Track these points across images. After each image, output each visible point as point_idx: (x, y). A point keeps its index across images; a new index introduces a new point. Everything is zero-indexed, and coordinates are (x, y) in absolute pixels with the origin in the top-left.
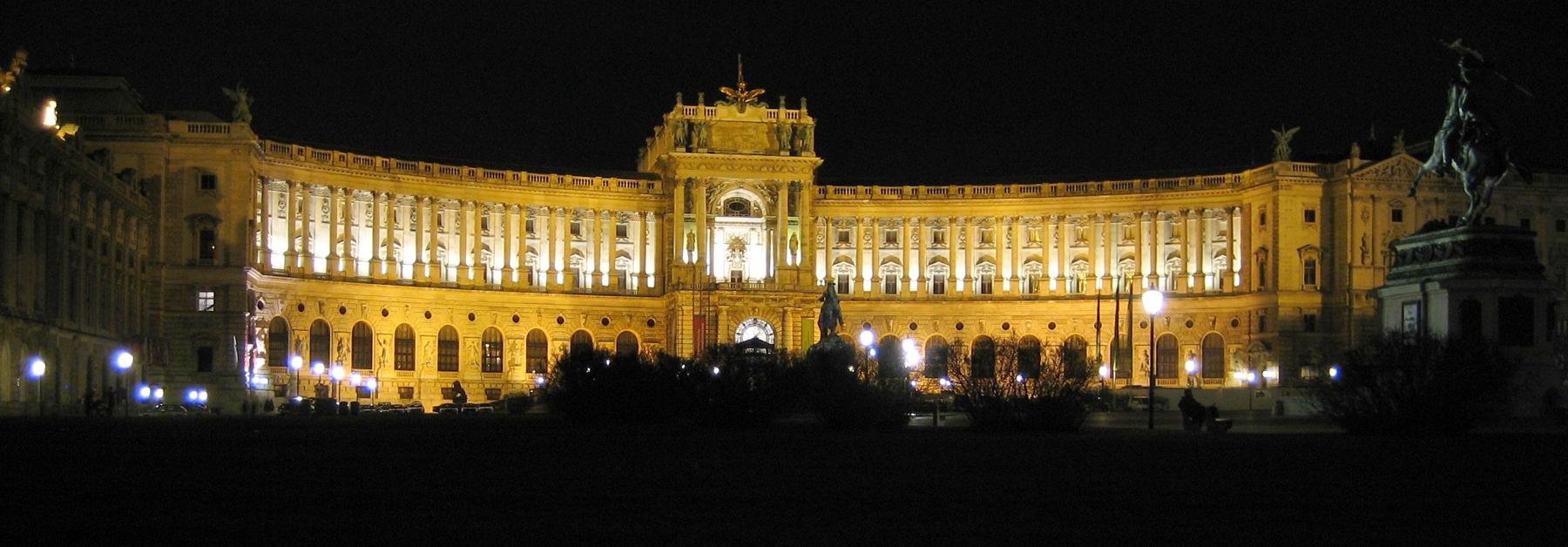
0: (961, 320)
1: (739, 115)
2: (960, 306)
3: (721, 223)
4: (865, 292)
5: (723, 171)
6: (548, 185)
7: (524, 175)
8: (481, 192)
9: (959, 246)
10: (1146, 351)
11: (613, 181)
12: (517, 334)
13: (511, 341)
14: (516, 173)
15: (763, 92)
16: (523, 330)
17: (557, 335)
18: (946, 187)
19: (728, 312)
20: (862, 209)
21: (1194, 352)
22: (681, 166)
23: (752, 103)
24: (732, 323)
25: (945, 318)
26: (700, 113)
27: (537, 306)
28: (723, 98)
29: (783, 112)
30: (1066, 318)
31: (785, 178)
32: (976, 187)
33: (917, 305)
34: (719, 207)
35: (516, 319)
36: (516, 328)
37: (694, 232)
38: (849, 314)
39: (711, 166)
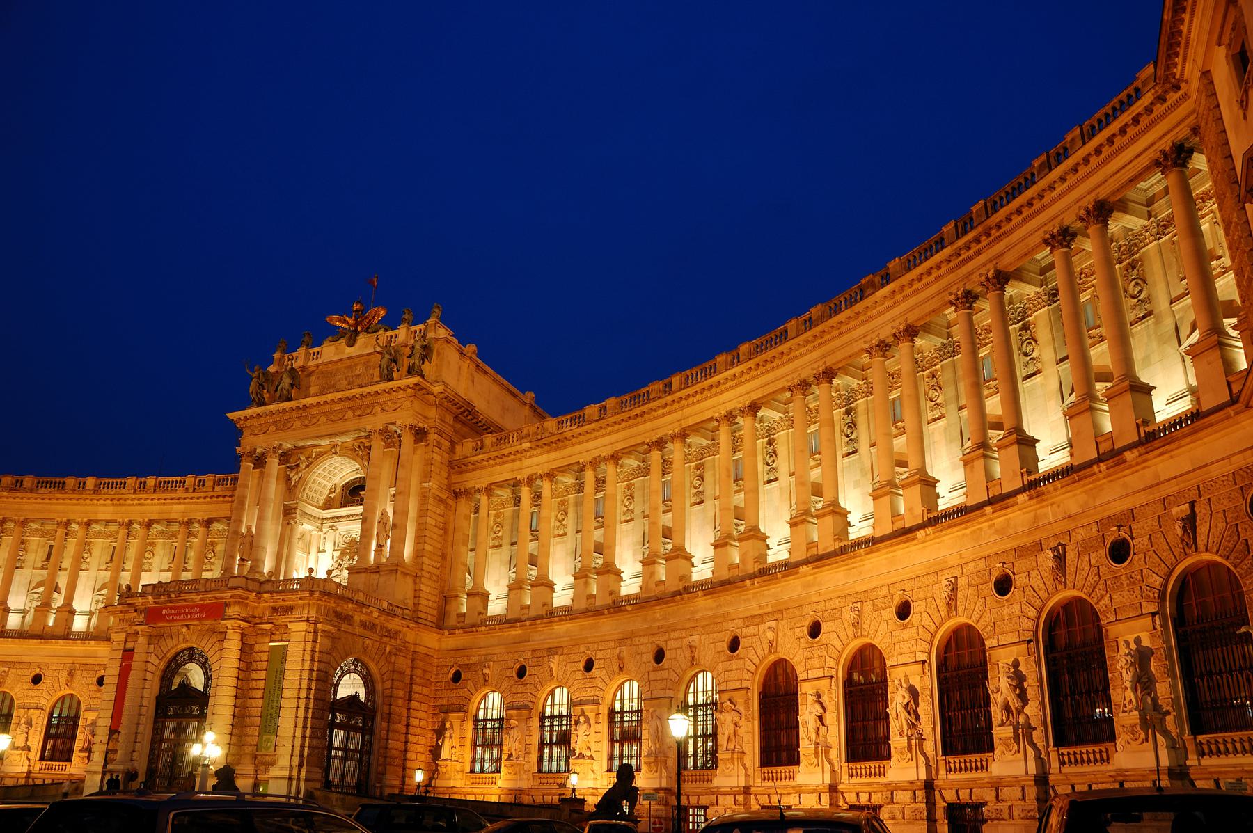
0: (659, 641)
1: (348, 350)
2: (658, 612)
3: (333, 518)
4: (523, 607)
5: (294, 430)
6: (124, 491)
7: (90, 482)
8: (25, 507)
9: (693, 500)
10: (1016, 664)
11: (209, 479)
12: (33, 702)
13: (22, 711)
14: (82, 480)
15: (382, 313)
16: (45, 697)
17: (94, 703)
18: (644, 390)
19: (150, 637)
20: (527, 462)
21: (1146, 642)
22: (246, 432)
23: (366, 330)
24: (153, 659)
25: (636, 641)
26: (300, 358)
27: (70, 660)
28: (336, 334)
29: (402, 334)
30: (837, 603)
31: (375, 421)
32: (688, 372)
33: (592, 621)
34: (332, 495)
35: (37, 680)
36: (34, 693)
37: (254, 530)
38: (497, 650)
39: (283, 425)
